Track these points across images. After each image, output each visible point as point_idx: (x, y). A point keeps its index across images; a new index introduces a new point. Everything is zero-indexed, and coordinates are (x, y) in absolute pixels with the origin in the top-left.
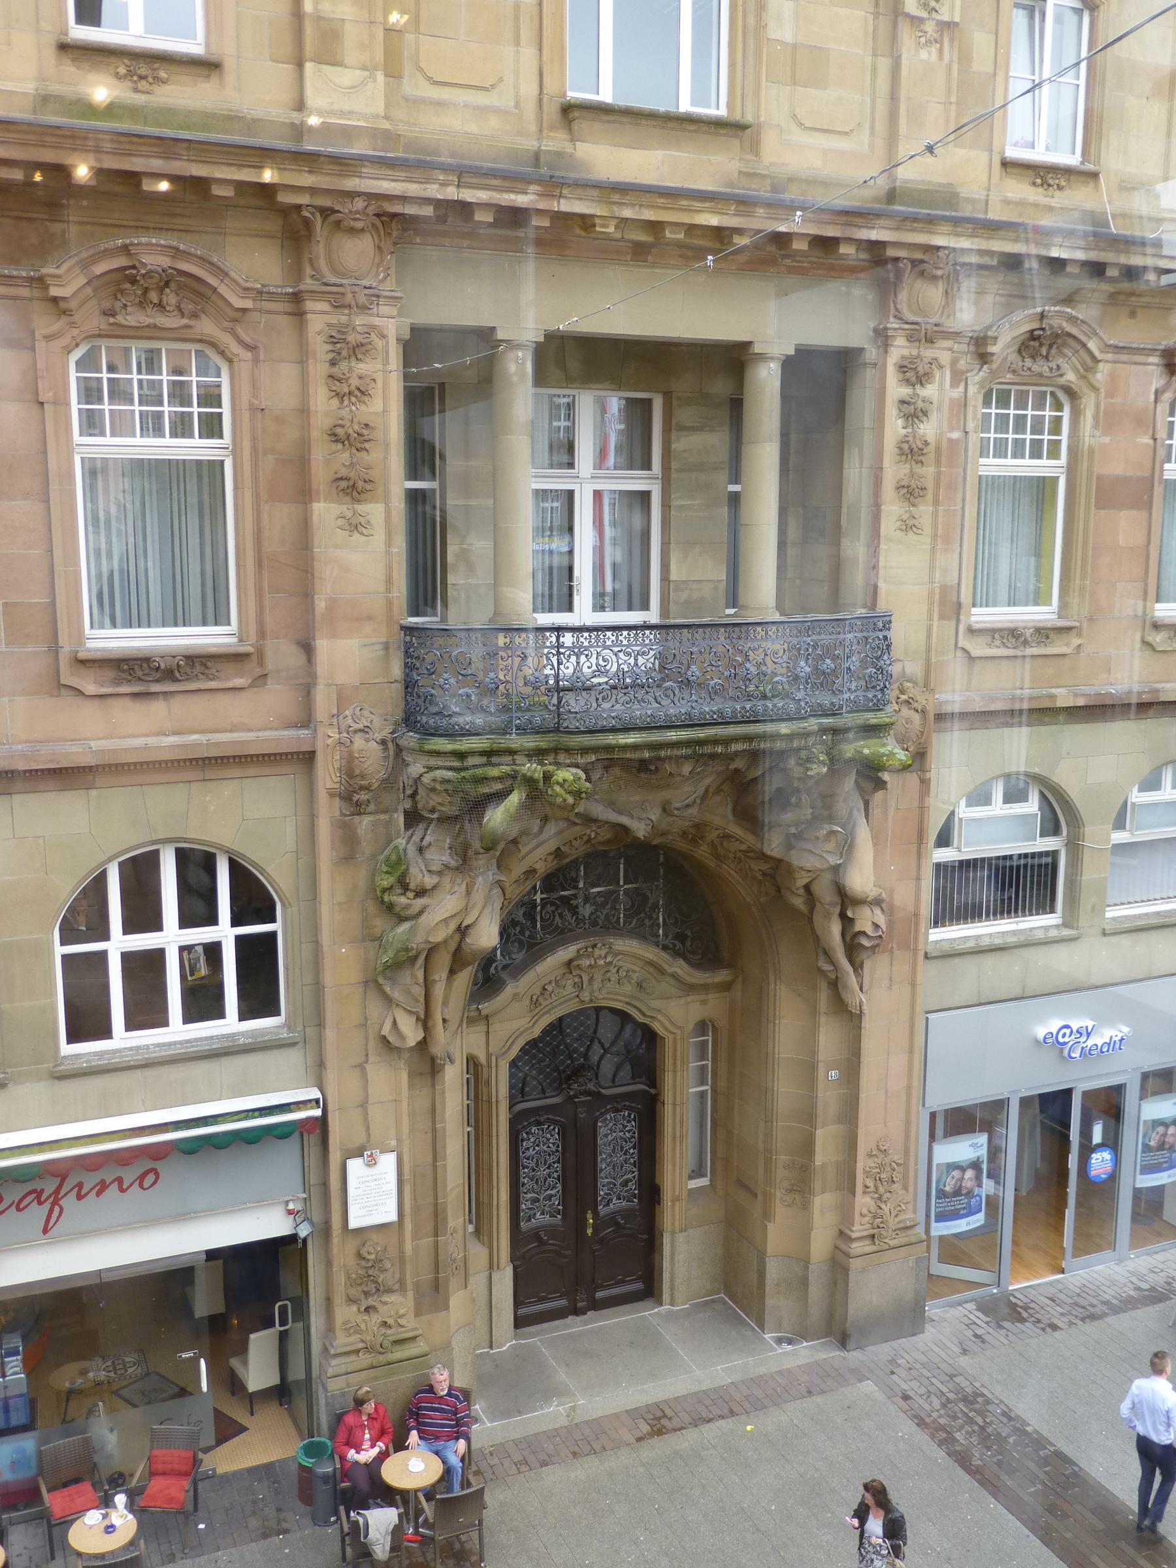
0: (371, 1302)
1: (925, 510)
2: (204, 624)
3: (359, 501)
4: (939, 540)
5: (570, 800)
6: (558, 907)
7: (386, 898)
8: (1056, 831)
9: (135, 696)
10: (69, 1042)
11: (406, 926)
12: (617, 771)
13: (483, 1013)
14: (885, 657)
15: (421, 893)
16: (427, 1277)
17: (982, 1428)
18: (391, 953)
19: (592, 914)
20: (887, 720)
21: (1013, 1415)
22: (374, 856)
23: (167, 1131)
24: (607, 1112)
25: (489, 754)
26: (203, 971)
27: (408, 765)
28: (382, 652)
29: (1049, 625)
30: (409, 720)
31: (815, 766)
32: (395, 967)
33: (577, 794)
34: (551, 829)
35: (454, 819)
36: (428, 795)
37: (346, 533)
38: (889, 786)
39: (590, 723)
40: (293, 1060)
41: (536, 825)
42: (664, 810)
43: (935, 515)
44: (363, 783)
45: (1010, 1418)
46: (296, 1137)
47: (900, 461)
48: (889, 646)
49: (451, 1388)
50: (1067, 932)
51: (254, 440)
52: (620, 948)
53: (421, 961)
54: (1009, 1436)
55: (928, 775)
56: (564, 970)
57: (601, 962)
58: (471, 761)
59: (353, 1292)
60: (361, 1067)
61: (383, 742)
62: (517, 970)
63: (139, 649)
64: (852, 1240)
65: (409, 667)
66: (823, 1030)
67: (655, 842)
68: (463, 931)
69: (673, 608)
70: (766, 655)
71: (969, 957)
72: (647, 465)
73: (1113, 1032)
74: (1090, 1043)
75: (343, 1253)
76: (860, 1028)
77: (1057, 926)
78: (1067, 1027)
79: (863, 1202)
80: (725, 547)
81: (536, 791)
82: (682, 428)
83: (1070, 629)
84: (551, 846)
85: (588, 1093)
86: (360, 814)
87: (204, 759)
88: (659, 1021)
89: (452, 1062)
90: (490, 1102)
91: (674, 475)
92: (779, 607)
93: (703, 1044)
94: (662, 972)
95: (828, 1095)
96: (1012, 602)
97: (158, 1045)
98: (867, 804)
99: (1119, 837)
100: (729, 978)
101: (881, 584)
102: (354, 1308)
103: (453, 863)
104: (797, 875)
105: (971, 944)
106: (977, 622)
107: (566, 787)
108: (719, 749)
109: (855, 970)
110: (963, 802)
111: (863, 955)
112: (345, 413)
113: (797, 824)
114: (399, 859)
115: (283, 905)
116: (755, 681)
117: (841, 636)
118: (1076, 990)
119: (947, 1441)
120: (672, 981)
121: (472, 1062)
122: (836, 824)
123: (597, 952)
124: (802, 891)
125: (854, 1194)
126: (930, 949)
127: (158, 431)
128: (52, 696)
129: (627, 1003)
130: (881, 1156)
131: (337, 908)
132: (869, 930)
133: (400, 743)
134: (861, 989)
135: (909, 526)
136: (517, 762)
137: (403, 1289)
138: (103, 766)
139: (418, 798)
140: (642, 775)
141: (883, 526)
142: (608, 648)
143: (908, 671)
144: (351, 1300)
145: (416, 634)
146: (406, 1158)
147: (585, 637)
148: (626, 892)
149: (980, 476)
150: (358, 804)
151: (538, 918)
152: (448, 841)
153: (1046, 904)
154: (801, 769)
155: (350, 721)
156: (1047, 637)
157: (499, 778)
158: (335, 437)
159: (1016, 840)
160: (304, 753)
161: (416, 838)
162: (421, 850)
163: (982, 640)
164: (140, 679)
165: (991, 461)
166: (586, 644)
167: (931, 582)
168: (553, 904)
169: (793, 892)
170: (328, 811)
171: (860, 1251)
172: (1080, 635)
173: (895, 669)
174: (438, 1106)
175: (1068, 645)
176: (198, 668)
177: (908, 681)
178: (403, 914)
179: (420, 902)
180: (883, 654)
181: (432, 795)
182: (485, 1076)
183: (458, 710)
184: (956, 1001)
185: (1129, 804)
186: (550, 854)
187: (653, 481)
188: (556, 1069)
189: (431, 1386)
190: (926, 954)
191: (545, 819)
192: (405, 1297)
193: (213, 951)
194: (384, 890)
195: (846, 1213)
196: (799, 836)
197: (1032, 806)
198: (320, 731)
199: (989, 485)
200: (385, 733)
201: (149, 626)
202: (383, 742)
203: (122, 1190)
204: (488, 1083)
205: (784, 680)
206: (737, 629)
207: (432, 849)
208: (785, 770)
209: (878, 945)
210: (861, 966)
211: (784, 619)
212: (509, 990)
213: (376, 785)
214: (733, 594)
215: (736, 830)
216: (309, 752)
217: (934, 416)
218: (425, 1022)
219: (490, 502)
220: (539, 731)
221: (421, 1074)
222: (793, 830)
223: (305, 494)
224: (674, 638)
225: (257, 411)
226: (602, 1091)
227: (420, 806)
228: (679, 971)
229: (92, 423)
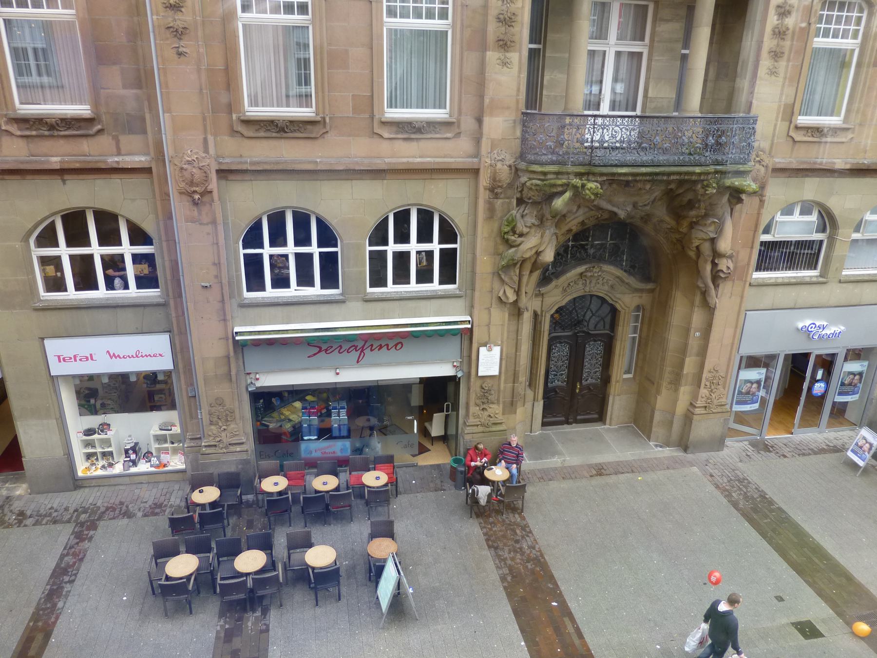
0: (484, 406)
1: (782, 64)
2: (435, 108)
3: (508, 51)
4: (787, 80)
5: (593, 197)
6: (579, 248)
7: (506, 237)
8: (824, 230)
9: (405, 139)
10: (371, 287)
11: (513, 250)
12: (614, 186)
13: (542, 292)
14: (752, 138)
15: (521, 235)
16: (509, 399)
17: (745, 493)
18: (506, 261)
19: (594, 253)
20: (749, 169)
21: (760, 489)
22: (501, 218)
23: (407, 327)
24: (591, 341)
25: (557, 173)
26: (425, 263)
27: (520, 177)
28: (513, 125)
29: (838, 126)
30: (522, 156)
31: (710, 189)
32: (507, 267)
33: (596, 195)
34: (581, 211)
35: (539, 203)
36: (528, 191)
37: (501, 67)
38: (744, 202)
39: (606, 161)
40: (460, 303)
41: (575, 209)
42: (634, 206)
43: (787, 67)
44: (500, 184)
45: (759, 491)
46: (459, 337)
47: (773, 38)
48: (755, 132)
49: (517, 444)
50: (821, 279)
51: (462, 20)
52: (607, 269)
53: (518, 266)
54: (758, 498)
55: (764, 198)
56: (578, 277)
57: (596, 275)
58: (549, 176)
59: (478, 401)
60: (489, 309)
61: (510, 166)
62: (557, 275)
63: (407, 118)
64: (695, 407)
65: (524, 132)
66: (695, 314)
67: (627, 221)
68: (538, 254)
69: (647, 110)
70: (693, 133)
71: (771, 287)
72: (642, 39)
73: (836, 329)
74: (824, 332)
75: (475, 385)
76: (714, 314)
77: (817, 276)
78: (814, 324)
79: (703, 392)
80: (676, 81)
81: (578, 192)
82: (662, 20)
83: (848, 129)
84: (580, 219)
85: (584, 332)
86: (497, 198)
87: (431, 169)
88: (619, 304)
89: (527, 310)
90: (540, 331)
91: (656, 44)
92: (701, 111)
93: (638, 316)
94: (623, 281)
95: (694, 342)
96: (819, 114)
97: (405, 292)
98: (732, 210)
99: (856, 236)
100: (653, 287)
101: (754, 101)
102: (478, 408)
103: (536, 223)
104: (694, 241)
105: (772, 281)
106: (800, 123)
107: (592, 190)
108: (665, 178)
109: (715, 288)
110: (779, 213)
111: (720, 281)
112: (504, 8)
113: (697, 217)
114: (513, 220)
115: (461, 237)
116: (687, 146)
117: (731, 126)
118: (821, 307)
119: (728, 496)
120: (627, 286)
121: (535, 314)
122: (717, 219)
123: (595, 270)
124: (695, 249)
125: (699, 387)
126: (752, 281)
127: (419, 16)
128: (370, 138)
129: (605, 294)
130: (715, 372)
131: (484, 240)
132: (725, 270)
133: (517, 167)
134: (717, 297)
135: (773, 72)
136: (571, 178)
137: (498, 403)
138: (390, 170)
139: (524, 192)
140: (626, 188)
141: (759, 72)
142: (618, 126)
143: (762, 146)
144: (477, 405)
145: (529, 116)
146: (504, 349)
147: (607, 121)
148: (610, 244)
149: (813, 48)
150: (497, 194)
151: (569, 252)
152: (535, 213)
153: (812, 265)
154: (703, 190)
155: (496, 156)
156: (836, 133)
157: (561, 185)
158: (499, 20)
159: (804, 234)
160: (474, 169)
161: (521, 211)
162: (522, 216)
163: (802, 132)
164: (407, 132)
165: (820, 39)
166: (608, 124)
167: (780, 101)
168: (577, 247)
169: (690, 249)
170: (483, 195)
171: (699, 412)
172: (853, 133)
173: (756, 145)
174: (520, 329)
175: (846, 137)
176: (432, 128)
177: (761, 151)
178: (512, 244)
179: (521, 239)
180: (751, 136)
181: (530, 192)
182: (540, 320)
183: (545, 152)
184: (762, 306)
185: (864, 220)
186: (579, 223)
187: (645, 47)
188: (571, 320)
189: (510, 442)
190: (750, 283)
191: (579, 207)
192: (499, 406)
193: (430, 254)
194: (505, 233)
195: (695, 396)
196: (696, 223)
197: (814, 218)
198: (483, 159)
199: (817, 51)
200: (511, 162)
201: (411, 108)
202: (510, 166)
203: (388, 349)
204: (541, 323)
205: (701, 146)
206: (681, 120)
207: (528, 216)
208: (695, 190)
209: (728, 277)
210: (718, 286)
211: (703, 115)
212: (554, 283)
213: (505, 186)
214: (679, 102)
215: (667, 219)
216: (477, 169)
217: (794, 14)
218: (518, 292)
219: (567, 55)
220: (582, 164)
221: (513, 315)
222: (694, 220)
223: (484, 48)
224: (649, 123)
225: (464, 6)
226: (590, 332)
227: (524, 196)
228: (631, 282)
229: (391, 13)
